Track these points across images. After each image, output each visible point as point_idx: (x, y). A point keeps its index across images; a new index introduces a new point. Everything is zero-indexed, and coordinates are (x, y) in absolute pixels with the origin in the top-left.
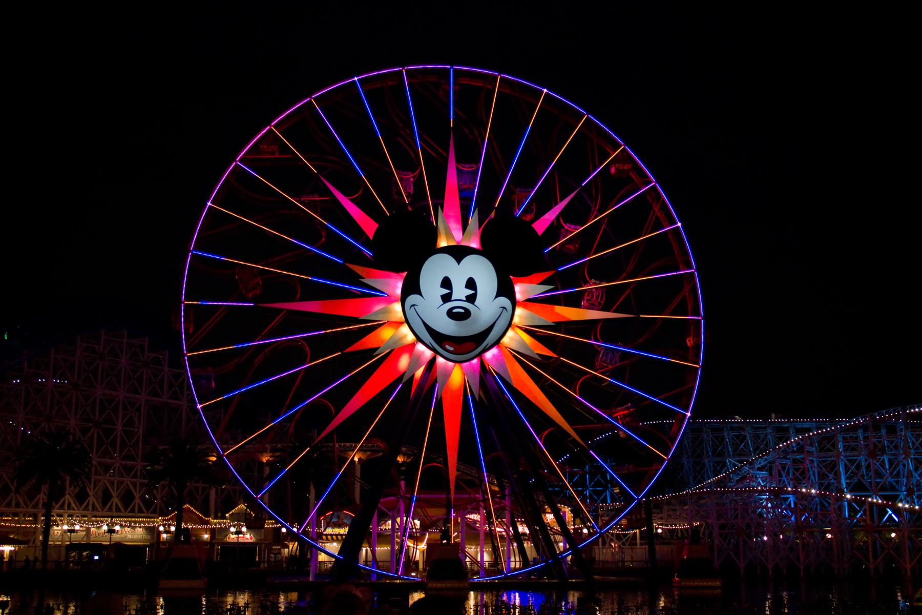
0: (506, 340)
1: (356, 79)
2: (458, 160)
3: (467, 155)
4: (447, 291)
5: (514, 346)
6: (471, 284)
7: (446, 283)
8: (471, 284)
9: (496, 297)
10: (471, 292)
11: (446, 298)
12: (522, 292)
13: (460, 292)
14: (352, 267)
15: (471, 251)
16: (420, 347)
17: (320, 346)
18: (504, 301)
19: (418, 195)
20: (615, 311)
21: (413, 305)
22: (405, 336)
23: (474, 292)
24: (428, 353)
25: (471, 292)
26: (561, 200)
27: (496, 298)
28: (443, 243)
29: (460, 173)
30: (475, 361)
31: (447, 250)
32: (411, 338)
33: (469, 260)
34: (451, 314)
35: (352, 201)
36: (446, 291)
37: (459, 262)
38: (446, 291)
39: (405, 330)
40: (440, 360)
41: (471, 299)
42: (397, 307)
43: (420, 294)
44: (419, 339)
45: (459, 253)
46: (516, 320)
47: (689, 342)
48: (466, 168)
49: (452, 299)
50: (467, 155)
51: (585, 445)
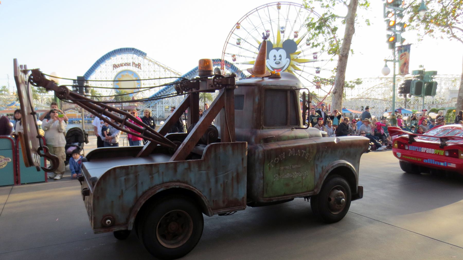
6: (280, 56)
7: (275, 56)
8: (280, 56)
10: (281, 58)
11: (275, 60)
13: (278, 58)
18: (288, 59)
23: (281, 58)
25: (280, 58)
27: (286, 58)
28: (274, 47)
34: (276, 63)
36: (275, 58)
37: (277, 51)
38: (275, 58)
41: (280, 59)
45: (277, 49)
49: (276, 59)
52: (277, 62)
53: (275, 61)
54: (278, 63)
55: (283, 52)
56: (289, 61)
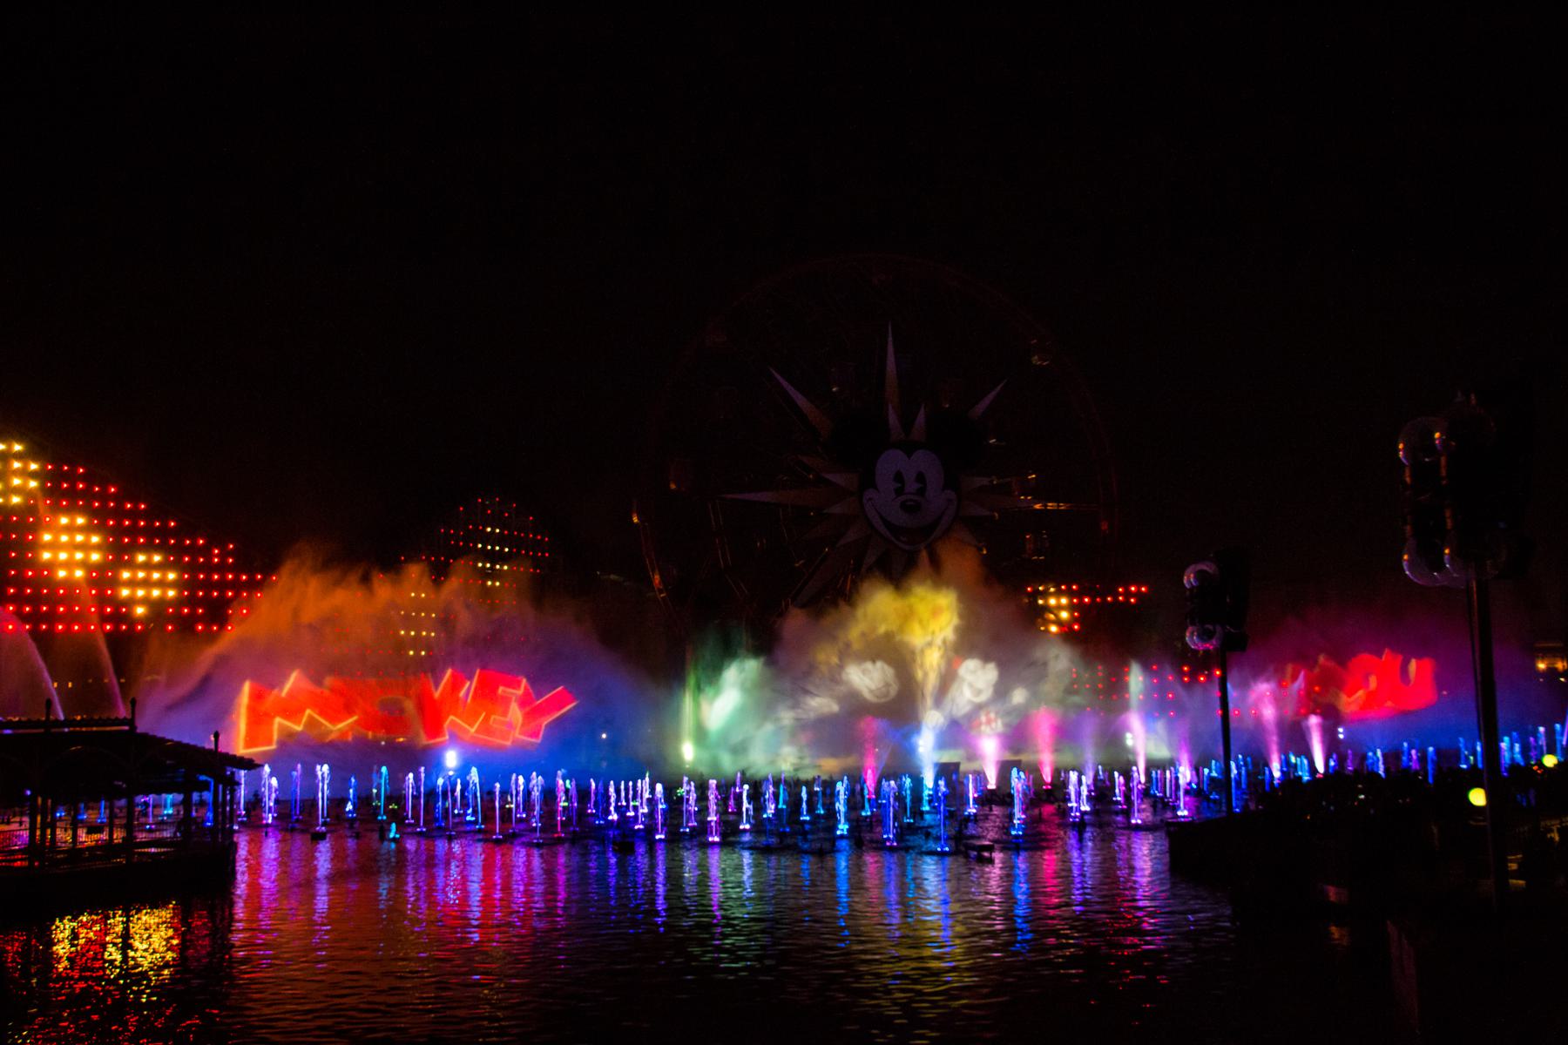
4: (899, 485)
6: (920, 478)
7: (899, 477)
8: (920, 478)
11: (899, 492)
13: (911, 486)
21: (870, 499)
23: (921, 485)
34: (904, 506)
37: (909, 457)
41: (921, 492)
43: (875, 487)
45: (909, 448)
52: (909, 503)
53: (903, 498)
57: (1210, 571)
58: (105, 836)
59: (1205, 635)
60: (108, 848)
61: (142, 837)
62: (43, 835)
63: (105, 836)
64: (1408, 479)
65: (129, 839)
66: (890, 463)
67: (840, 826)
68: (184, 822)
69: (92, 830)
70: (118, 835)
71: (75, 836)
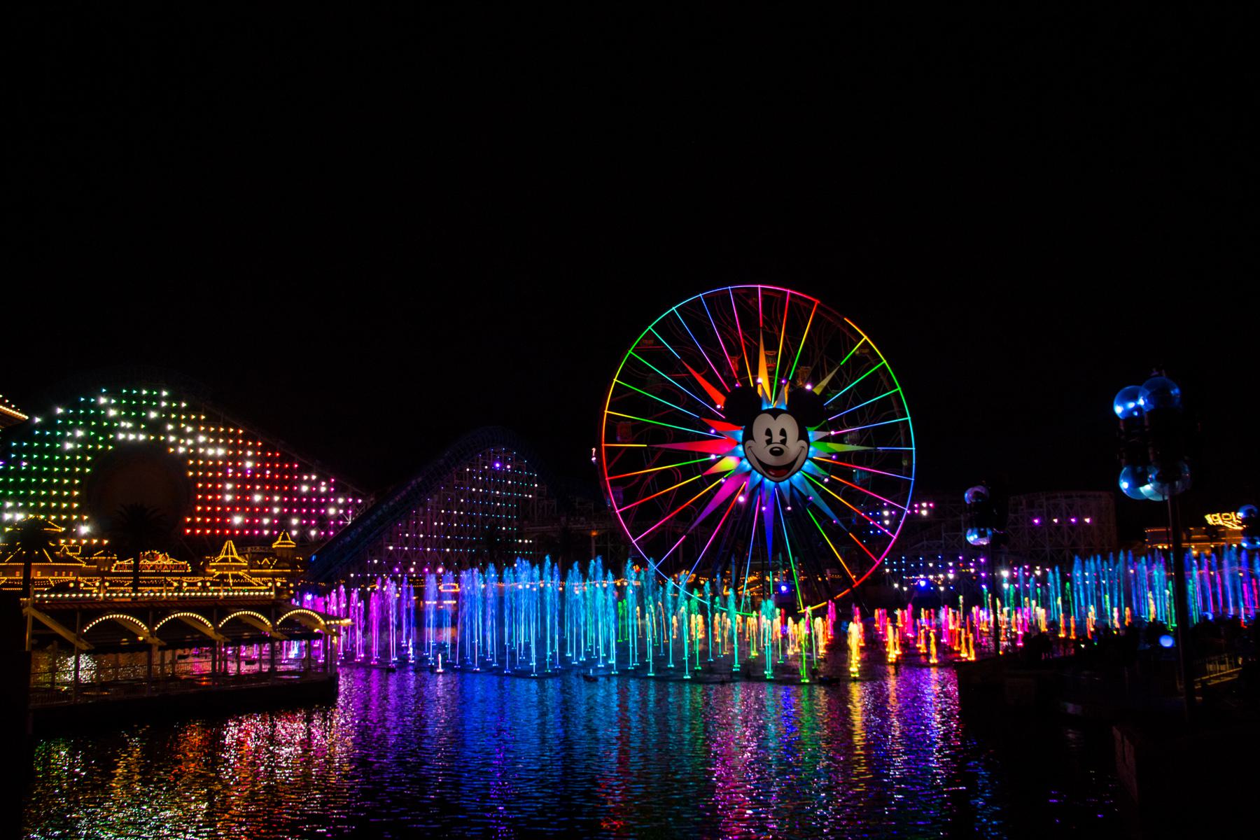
0: (805, 467)
1: (700, 295)
2: (765, 350)
3: (771, 345)
5: (809, 470)
8: (783, 432)
9: (799, 439)
10: (783, 438)
11: (769, 442)
12: (813, 437)
13: (777, 438)
14: (705, 420)
15: (781, 412)
16: (754, 472)
17: (688, 472)
18: (803, 443)
19: (743, 372)
20: (862, 445)
22: (745, 467)
24: (759, 477)
25: (783, 438)
26: (828, 375)
28: (765, 407)
29: (767, 357)
30: (787, 482)
31: (768, 411)
32: (749, 467)
33: (782, 417)
34: (772, 452)
35: (702, 376)
36: (769, 437)
37: (775, 418)
38: (769, 437)
39: (745, 462)
40: (767, 481)
41: (783, 442)
42: (740, 448)
43: (753, 439)
44: (754, 468)
45: (775, 413)
46: (810, 455)
47: (905, 463)
48: (769, 353)
50: (771, 345)
51: (843, 526)
54: (777, 453)
55: (788, 423)
56: (806, 447)
57: (983, 492)
58: (256, 667)
59: (981, 535)
60: (259, 674)
61: (281, 668)
62: (220, 665)
63: (256, 667)
64: (1122, 428)
65: (272, 670)
66: (762, 423)
67: (735, 666)
68: (307, 661)
69: (250, 662)
70: (266, 668)
71: (239, 667)
